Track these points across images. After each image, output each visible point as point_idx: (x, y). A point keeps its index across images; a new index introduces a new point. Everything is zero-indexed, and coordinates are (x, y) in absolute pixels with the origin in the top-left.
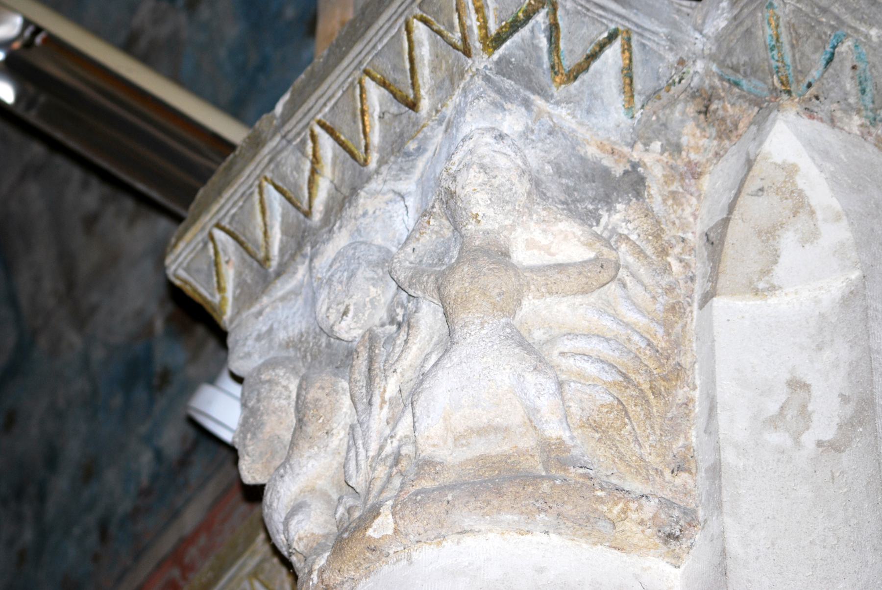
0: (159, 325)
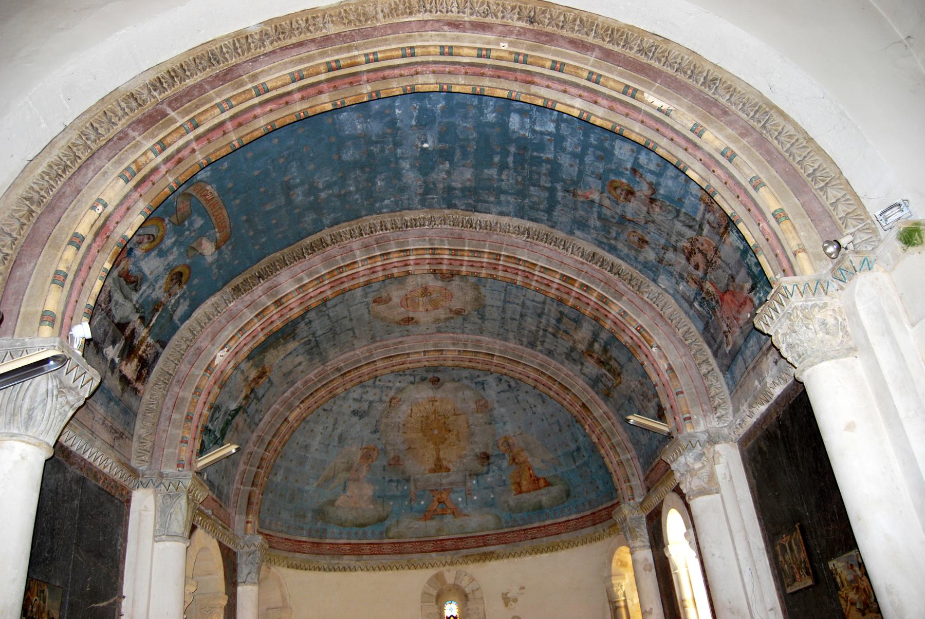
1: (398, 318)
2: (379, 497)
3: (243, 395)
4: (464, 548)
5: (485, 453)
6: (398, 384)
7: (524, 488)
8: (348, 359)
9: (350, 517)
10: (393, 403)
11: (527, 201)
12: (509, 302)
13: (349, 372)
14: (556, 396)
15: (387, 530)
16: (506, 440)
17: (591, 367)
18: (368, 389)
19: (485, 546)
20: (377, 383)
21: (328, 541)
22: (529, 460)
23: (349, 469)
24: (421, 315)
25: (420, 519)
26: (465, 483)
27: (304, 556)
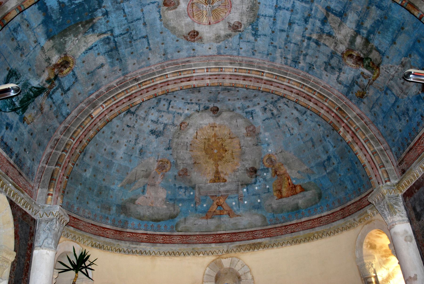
0: (420, 92)
1: (185, 31)
2: (171, 200)
3: (45, 76)
4: (237, 241)
5: (253, 168)
6: (186, 112)
7: (284, 194)
8: (145, 72)
9: (148, 213)
10: (182, 127)
12: (280, 8)
13: (145, 82)
14: (315, 106)
15: (177, 225)
16: (270, 158)
17: (350, 71)
18: (163, 114)
19: (254, 239)
20: (170, 109)
21: (128, 230)
22: (288, 172)
23: (147, 176)
24: (205, 31)
25: (202, 218)
26: (237, 191)
27: (107, 240)
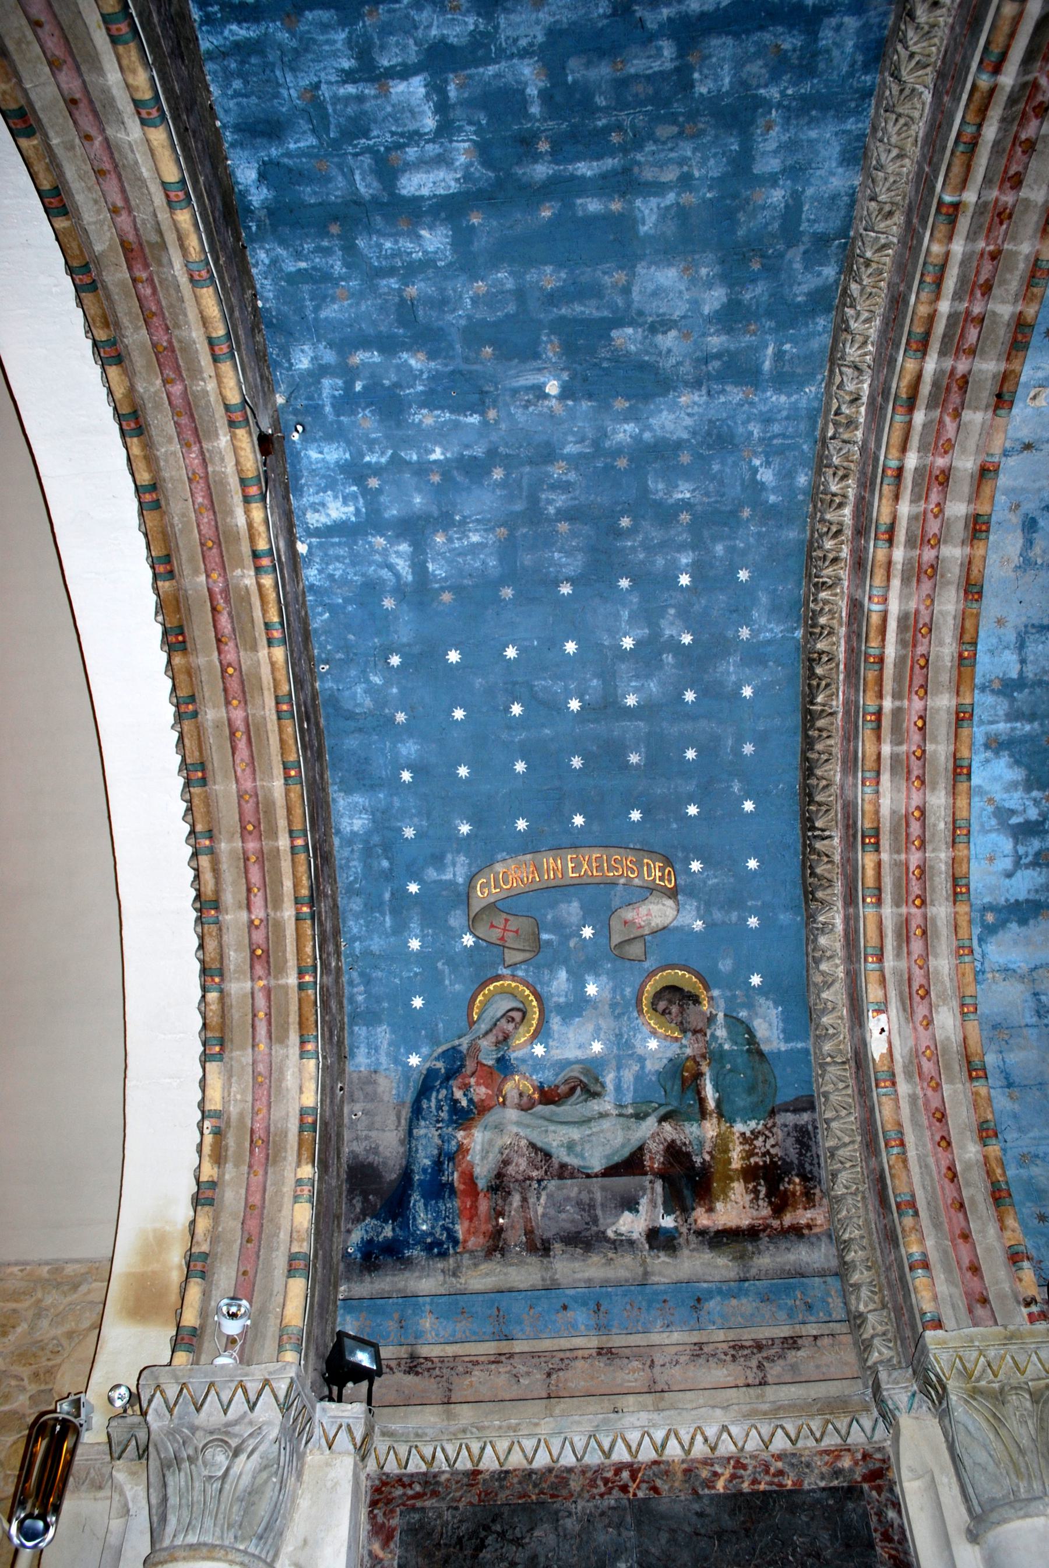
11: (773, 93)
